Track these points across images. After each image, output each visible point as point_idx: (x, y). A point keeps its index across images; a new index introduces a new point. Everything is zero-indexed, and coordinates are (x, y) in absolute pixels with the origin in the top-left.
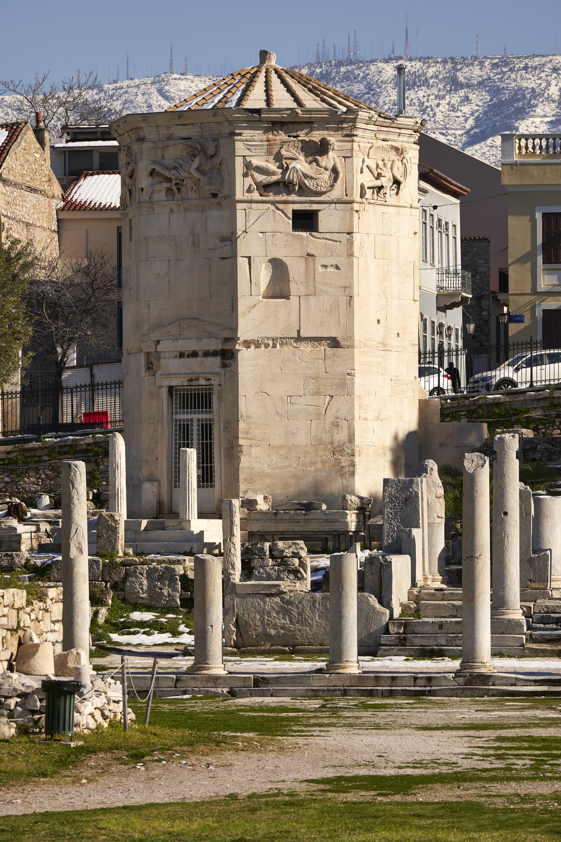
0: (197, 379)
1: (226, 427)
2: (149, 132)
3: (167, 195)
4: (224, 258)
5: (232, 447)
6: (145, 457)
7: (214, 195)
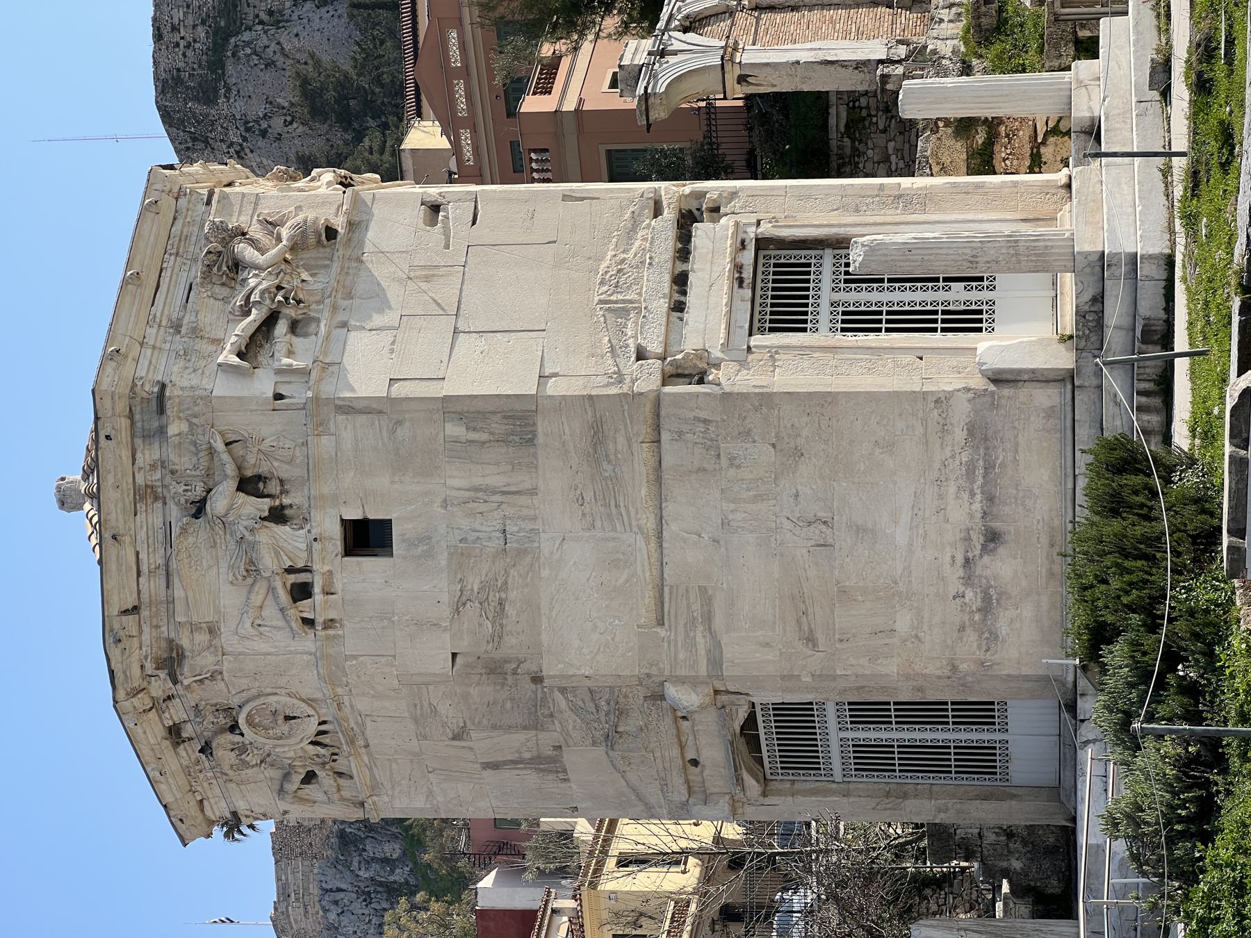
1: (857, 211)
2: (152, 368)
3: (306, 335)
4: (474, 223)
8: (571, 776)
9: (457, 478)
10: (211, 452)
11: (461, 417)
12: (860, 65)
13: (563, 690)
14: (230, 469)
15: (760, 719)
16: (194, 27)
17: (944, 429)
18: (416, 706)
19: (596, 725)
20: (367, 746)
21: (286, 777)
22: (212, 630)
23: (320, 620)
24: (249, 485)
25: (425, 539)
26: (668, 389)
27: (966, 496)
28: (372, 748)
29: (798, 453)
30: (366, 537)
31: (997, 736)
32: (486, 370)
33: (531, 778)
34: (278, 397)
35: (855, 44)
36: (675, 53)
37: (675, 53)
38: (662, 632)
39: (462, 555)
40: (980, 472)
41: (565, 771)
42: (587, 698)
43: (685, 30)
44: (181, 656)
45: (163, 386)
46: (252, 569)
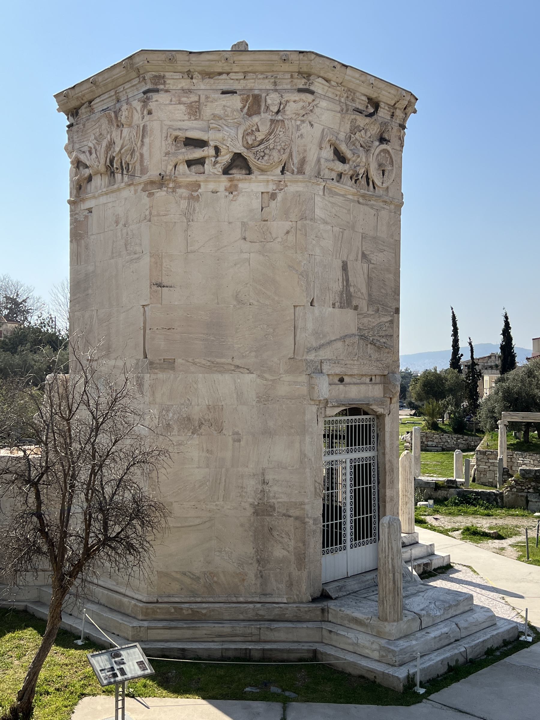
8: (337, 310)
13: (391, 322)
15: (357, 417)
18: (384, 242)
19: (371, 333)
20: (359, 202)
28: (357, 205)
31: (348, 543)
33: (337, 286)
41: (341, 307)
42: (387, 333)
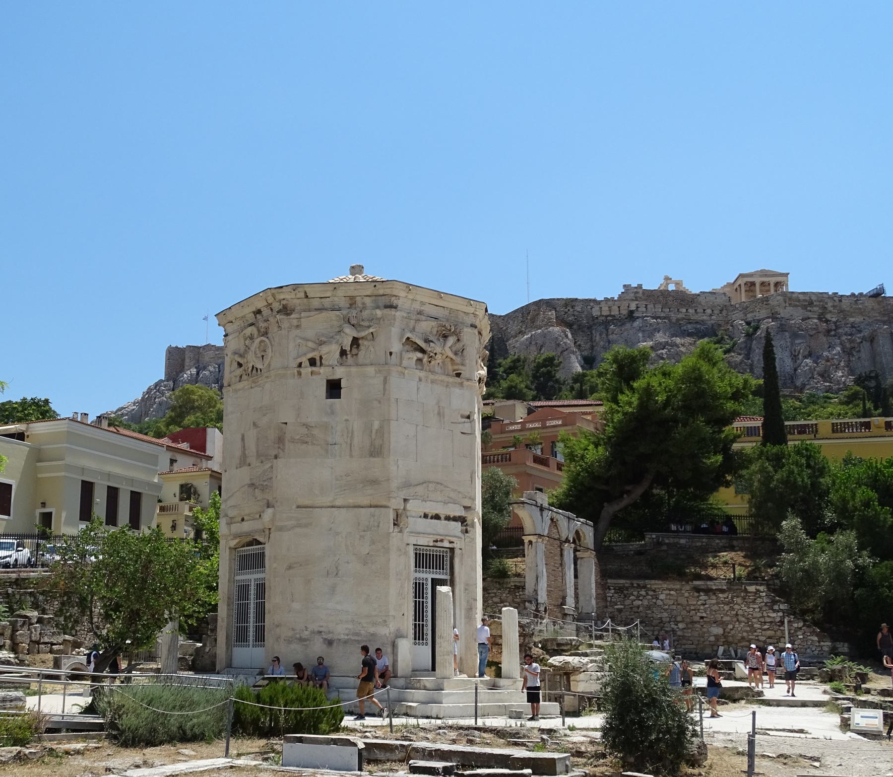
0: (442, 541)
1: (466, 589)
3: (416, 364)
5: (471, 609)
6: (392, 613)
7: (458, 375)
8: (238, 470)
9: (357, 425)
10: (369, 327)
11: (381, 427)
12: (536, 591)
13: (272, 467)
14: (362, 334)
16: (574, 315)
17: (375, 624)
21: (241, 356)
22: (298, 327)
23: (302, 370)
24: (355, 342)
25: (333, 413)
26: (391, 510)
27: (347, 632)
29: (365, 563)
30: (334, 388)
32: (400, 435)
34: (391, 354)
35: (545, 589)
36: (542, 515)
37: (542, 515)
38: (294, 507)
39: (326, 427)
40: (356, 638)
43: (552, 519)
44: (288, 314)
45: (396, 307)
46: (322, 343)
